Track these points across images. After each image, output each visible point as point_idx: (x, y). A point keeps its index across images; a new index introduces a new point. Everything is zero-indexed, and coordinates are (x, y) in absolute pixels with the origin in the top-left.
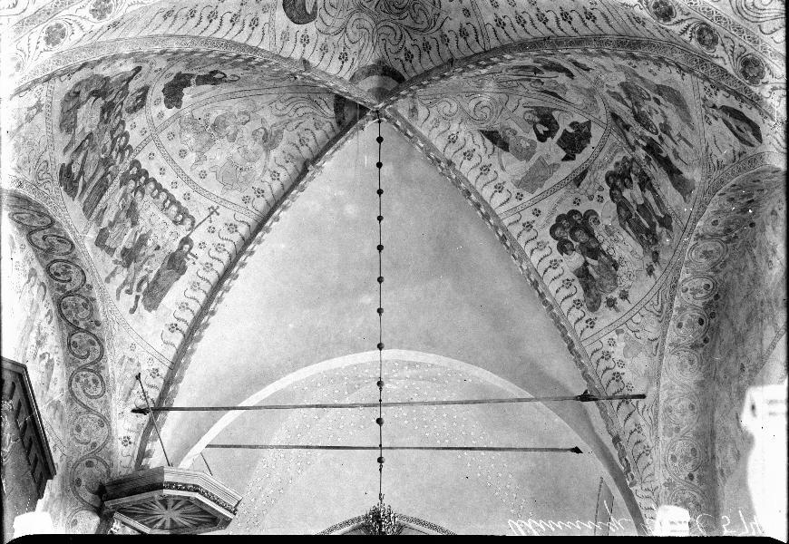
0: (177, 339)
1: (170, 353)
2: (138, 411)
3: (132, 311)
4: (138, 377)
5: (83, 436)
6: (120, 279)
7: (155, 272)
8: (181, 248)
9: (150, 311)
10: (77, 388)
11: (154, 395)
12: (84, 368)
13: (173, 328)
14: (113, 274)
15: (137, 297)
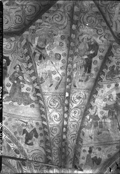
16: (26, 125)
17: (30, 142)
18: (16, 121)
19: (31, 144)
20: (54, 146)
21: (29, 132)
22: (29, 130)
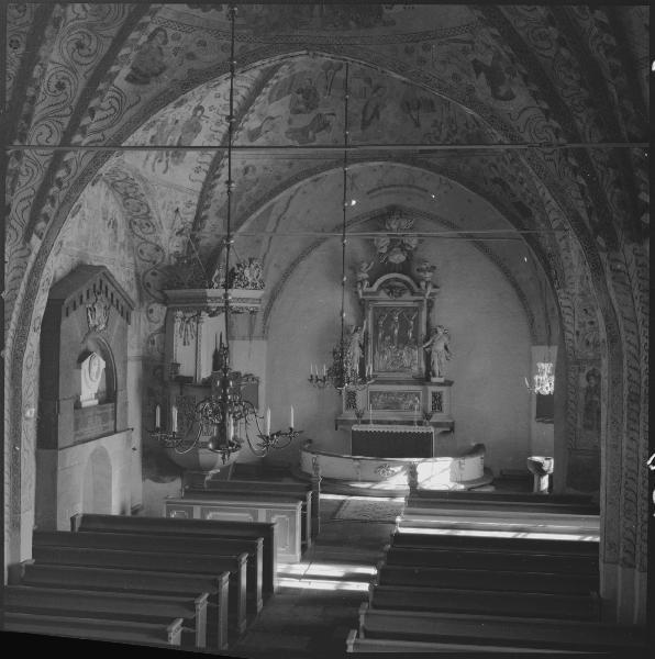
0: (202, 176)
1: (198, 187)
2: (180, 233)
3: (165, 172)
4: (177, 210)
5: (145, 257)
6: (152, 158)
7: (177, 138)
8: (195, 115)
9: (176, 163)
10: (136, 228)
11: (191, 218)
12: (137, 217)
13: (197, 171)
14: (147, 159)
15: (167, 162)
16: (473, 49)
17: (503, 91)
18: (444, 46)
19: (510, 97)
20: (566, 87)
21: (489, 64)
22: (488, 59)
